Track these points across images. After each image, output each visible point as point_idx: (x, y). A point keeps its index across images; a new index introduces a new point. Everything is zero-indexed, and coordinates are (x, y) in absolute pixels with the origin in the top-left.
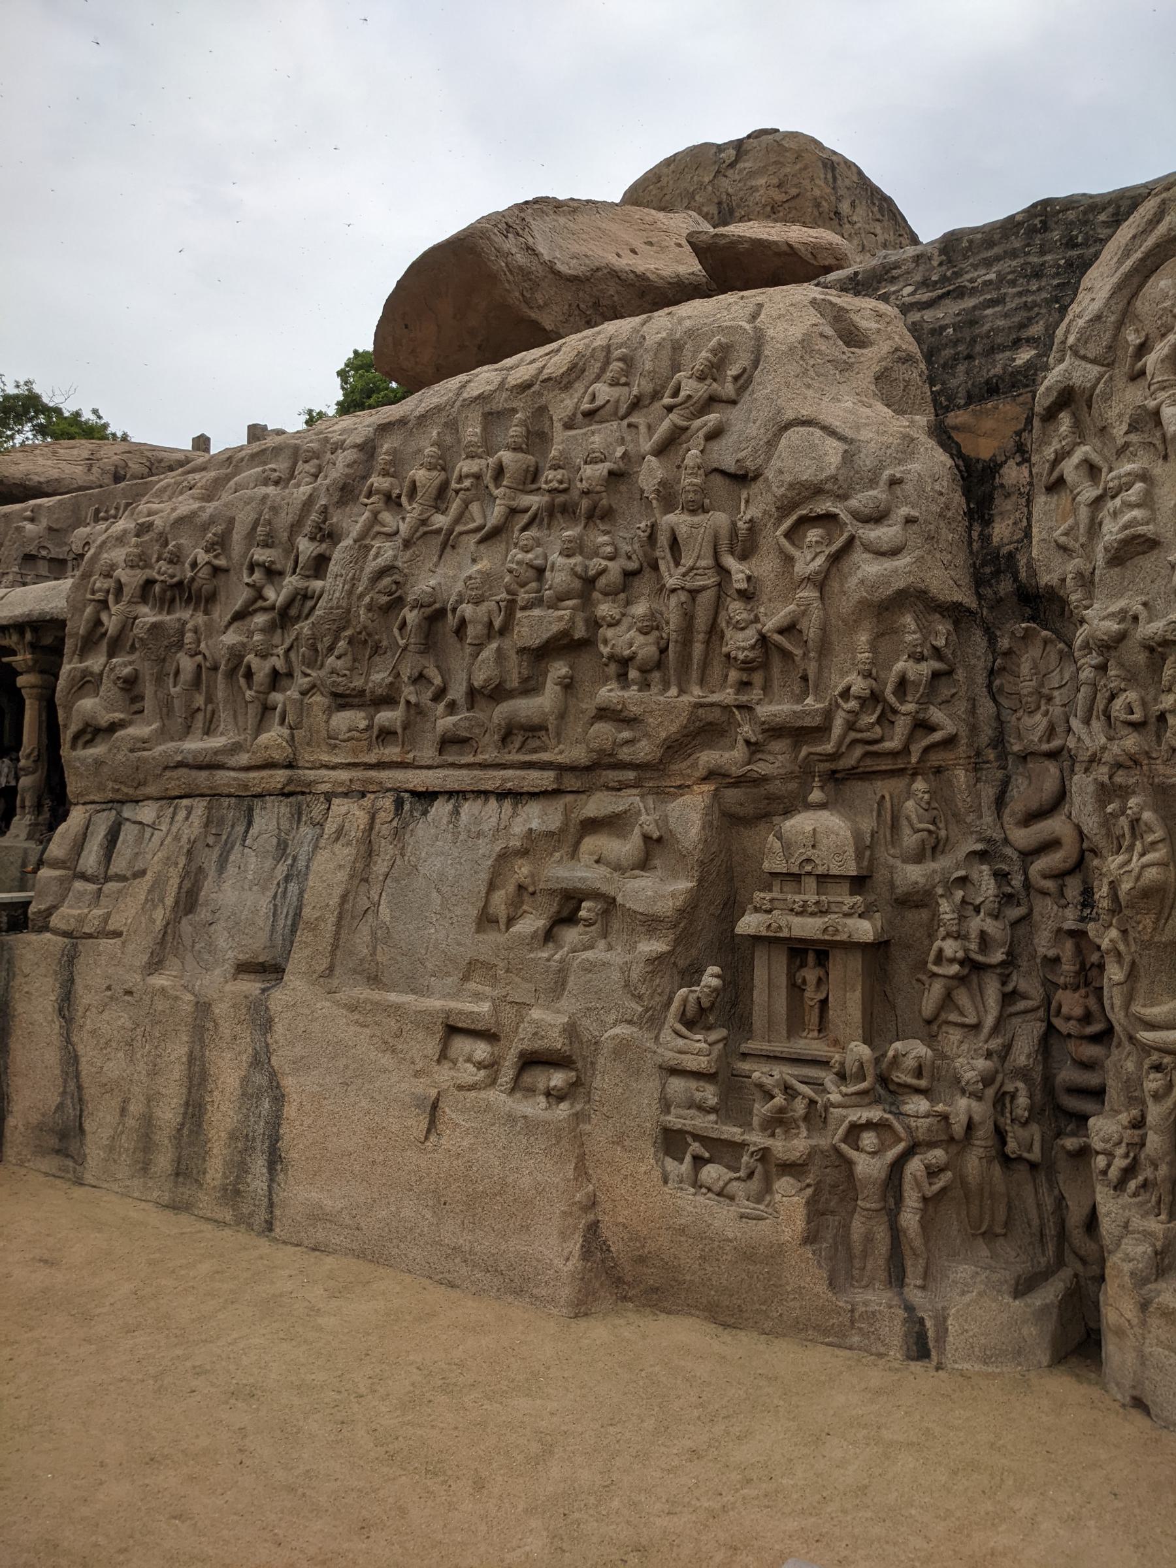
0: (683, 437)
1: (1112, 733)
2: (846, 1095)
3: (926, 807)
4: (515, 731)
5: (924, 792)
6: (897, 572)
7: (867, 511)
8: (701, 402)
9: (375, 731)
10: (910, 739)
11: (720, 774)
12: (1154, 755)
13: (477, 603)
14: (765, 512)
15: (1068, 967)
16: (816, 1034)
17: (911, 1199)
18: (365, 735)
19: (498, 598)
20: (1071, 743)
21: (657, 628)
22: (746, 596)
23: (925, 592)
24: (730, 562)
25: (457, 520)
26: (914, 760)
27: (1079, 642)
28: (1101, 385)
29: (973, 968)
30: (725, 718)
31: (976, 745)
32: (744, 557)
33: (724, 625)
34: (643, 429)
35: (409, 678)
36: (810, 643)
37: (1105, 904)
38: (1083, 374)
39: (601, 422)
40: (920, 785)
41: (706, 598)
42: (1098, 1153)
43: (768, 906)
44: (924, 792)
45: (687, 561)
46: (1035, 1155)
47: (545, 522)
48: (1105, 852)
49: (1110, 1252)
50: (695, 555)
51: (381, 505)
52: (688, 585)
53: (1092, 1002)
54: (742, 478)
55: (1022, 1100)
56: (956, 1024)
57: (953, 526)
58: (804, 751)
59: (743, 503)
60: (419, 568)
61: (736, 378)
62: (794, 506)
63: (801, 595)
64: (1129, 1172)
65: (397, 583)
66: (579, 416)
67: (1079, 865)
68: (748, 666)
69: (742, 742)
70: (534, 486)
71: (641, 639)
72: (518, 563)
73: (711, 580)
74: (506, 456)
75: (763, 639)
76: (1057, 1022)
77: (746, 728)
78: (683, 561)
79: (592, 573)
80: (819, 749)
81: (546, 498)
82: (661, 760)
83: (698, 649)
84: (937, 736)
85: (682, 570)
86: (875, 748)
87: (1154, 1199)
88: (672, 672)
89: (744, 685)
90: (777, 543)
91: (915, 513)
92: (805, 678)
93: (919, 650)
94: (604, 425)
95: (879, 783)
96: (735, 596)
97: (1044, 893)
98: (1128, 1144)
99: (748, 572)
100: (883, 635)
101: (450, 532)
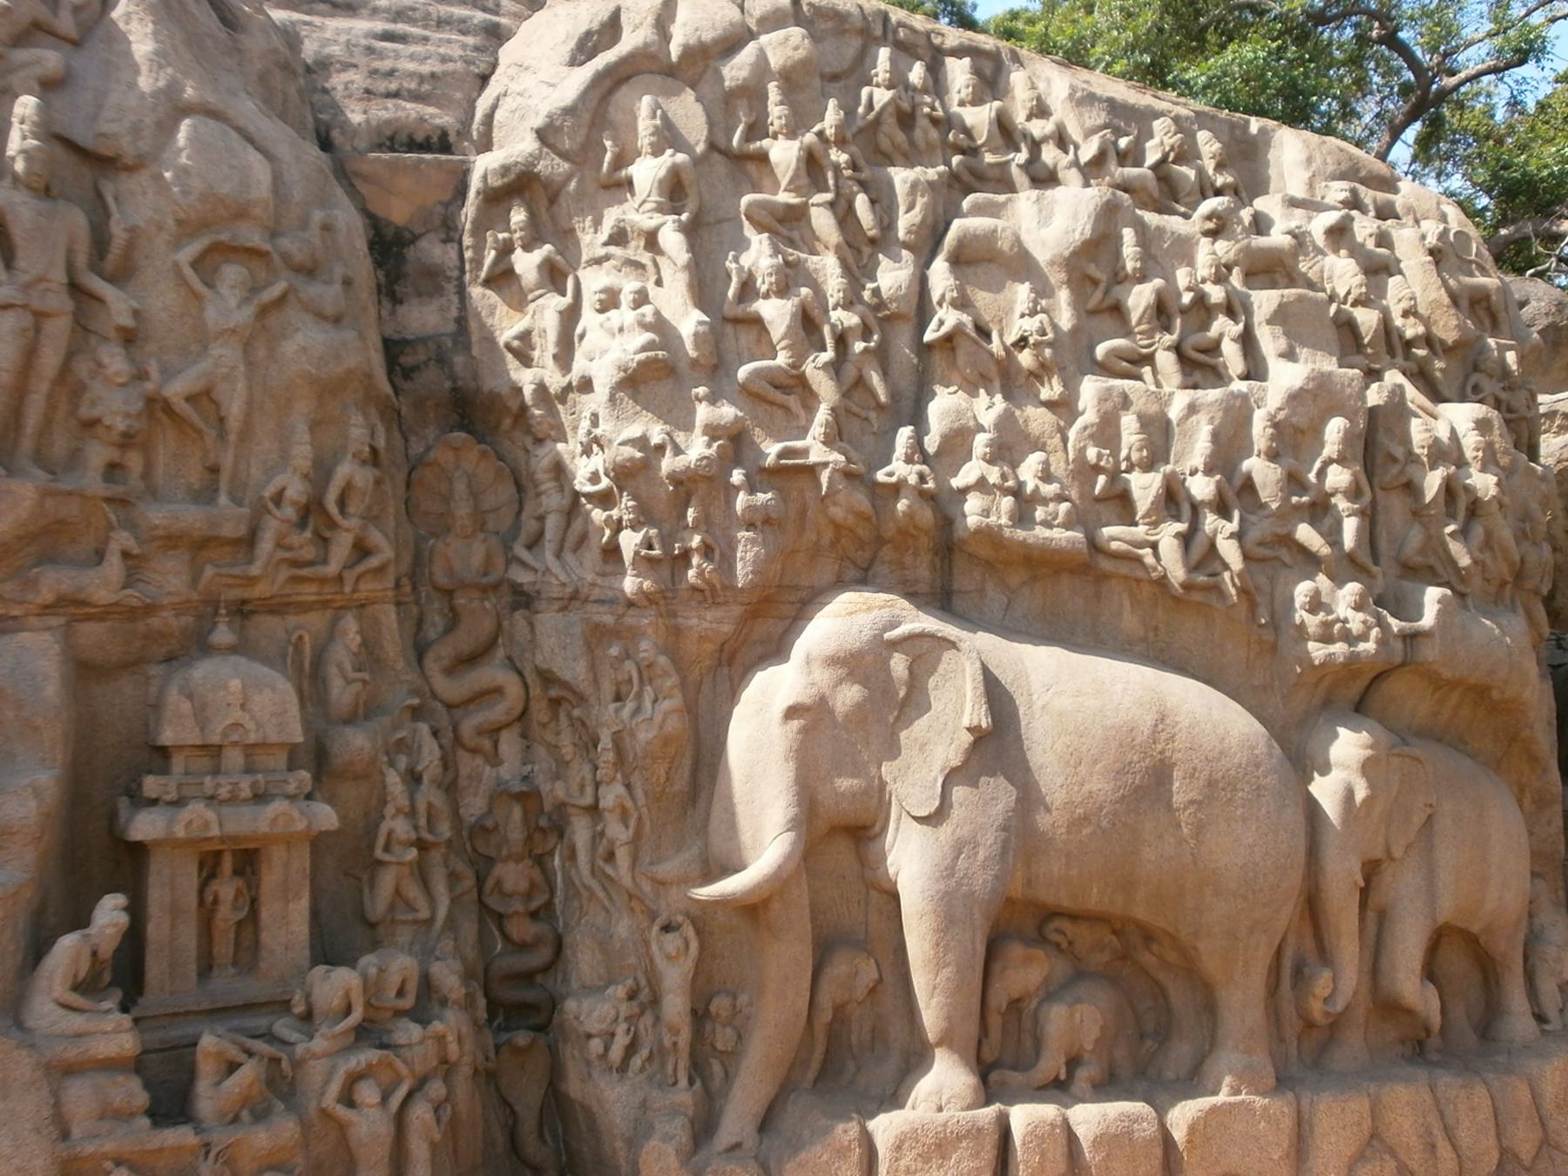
1: (609, 568)
2: (334, 1037)
7: (299, 257)
12: (670, 595)
15: (516, 834)
16: (232, 970)
17: (419, 1150)
20: (523, 577)
26: (347, 589)
27: (546, 462)
28: (573, 185)
29: (422, 845)
32: (112, 279)
37: (610, 756)
38: (552, 166)
42: (589, 1036)
43: (173, 796)
46: (490, 1065)
48: (592, 700)
49: (634, 1143)
52: (36, 304)
53: (536, 874)
55: (482, 1002)
56: (404, 922)
62: (203, 226)
64: (631, 1049)
67: (524, 714)
68: (127, 441)
69: (118, 554)
75: (157, 406)
76: (493, 902)
77: (125, 534)
78: (21, 263)
80: (236, 571)
85: (26, 278)
86: (305, 572)
87: (670, 1068)
89: (113, 470)
92: (214, 470)
95: (293, 620)
96: (112, 334)
97: (474, 751)
98: (627, 1019)
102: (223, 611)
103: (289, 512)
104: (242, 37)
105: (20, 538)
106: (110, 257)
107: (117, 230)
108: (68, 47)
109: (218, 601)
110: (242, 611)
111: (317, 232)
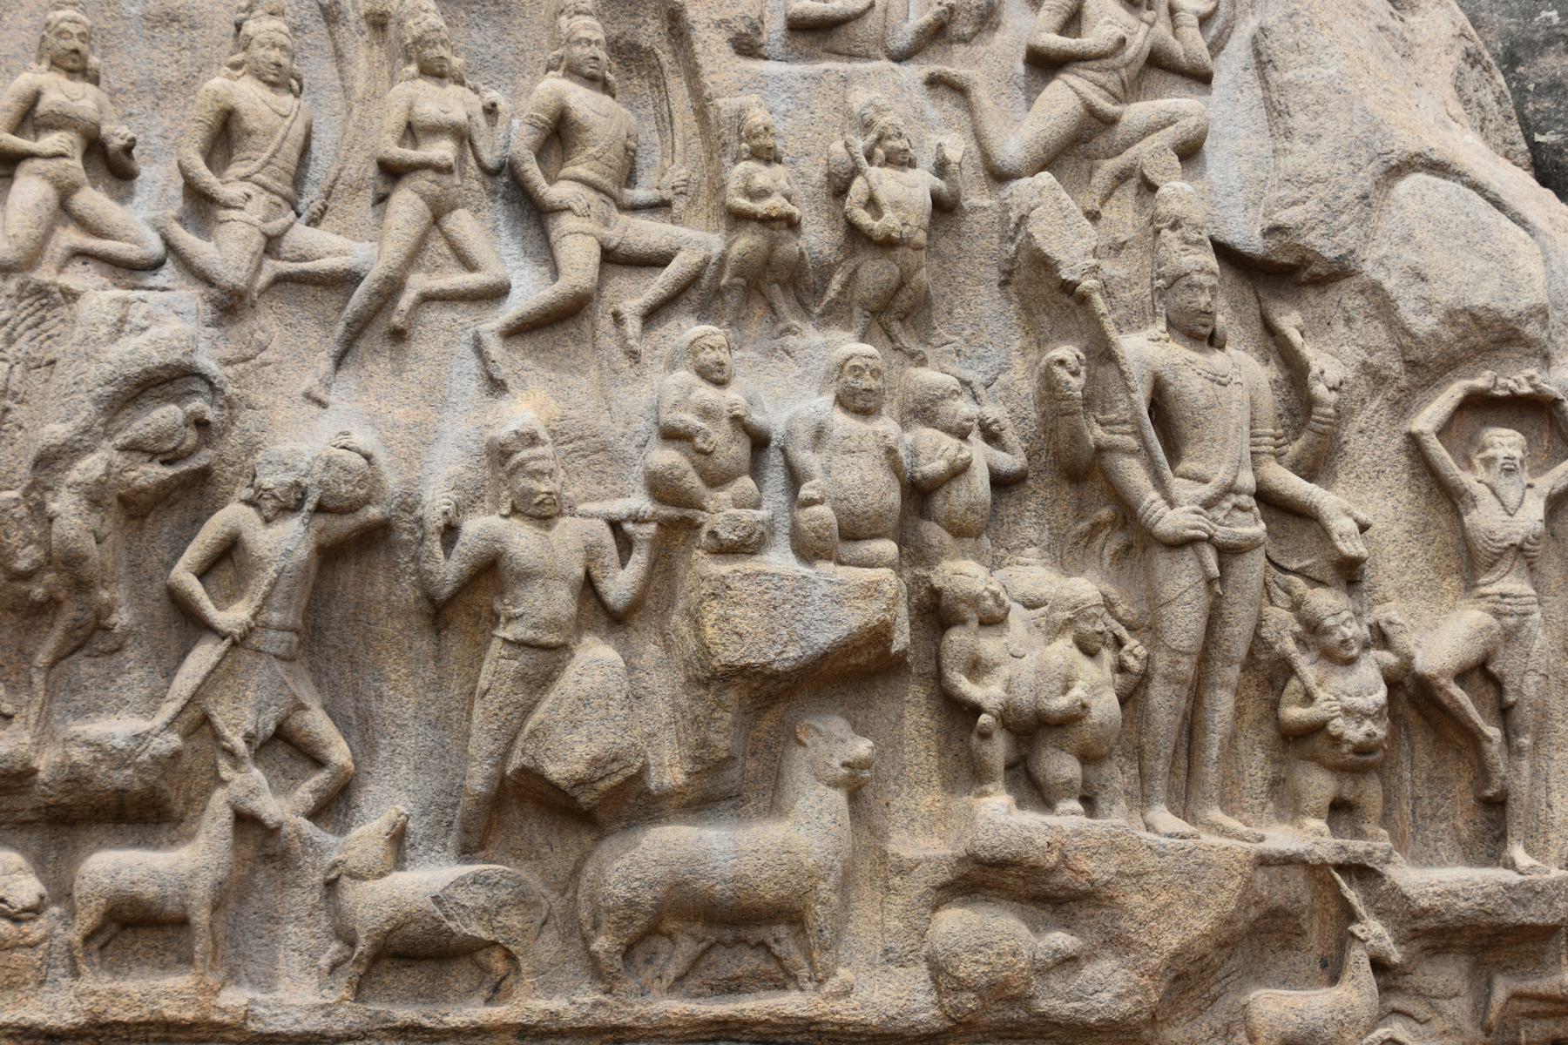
0: (1102, 142)
4: (670, 925)
8: (1141, 62)
9: (87, 919)
13: (543, 514)
18: (35, 930)
19: (619, 507)
22: (1349, 573)
25: (414, 257)
32: (1310, 475)
33: (1290, 645)
34: (981, 94)
35: (249, 738)
36: (1526, 714)
39: (851, 56)
41: (1253, 568)
47: (732, 300)
51: (74, 166)
52: (1221, 533)
54: (1273, 273)
58: (1502, 989)
59: (1296, 338)
60: (268, 384)
61: (1204, 20)
65: (201, 424)
66: (774, 29)
68: (1361, 762)
70: (640, 194)
71: (1085, 664)
72: (706, 413)
73: (1259, 529)
74: (583, 101)
75: (1411, 694)
79: (934, 466)
81: (747, 242)
83: (1222, 705)
85: (1206, 491)
88: (1161, 766)
89: (1340, 810)
94: (861, 66)
96: (1329, 575)
99: (1363, 516)
101: (391, 289)
104: (1411, 19)
105: (1221, 946)
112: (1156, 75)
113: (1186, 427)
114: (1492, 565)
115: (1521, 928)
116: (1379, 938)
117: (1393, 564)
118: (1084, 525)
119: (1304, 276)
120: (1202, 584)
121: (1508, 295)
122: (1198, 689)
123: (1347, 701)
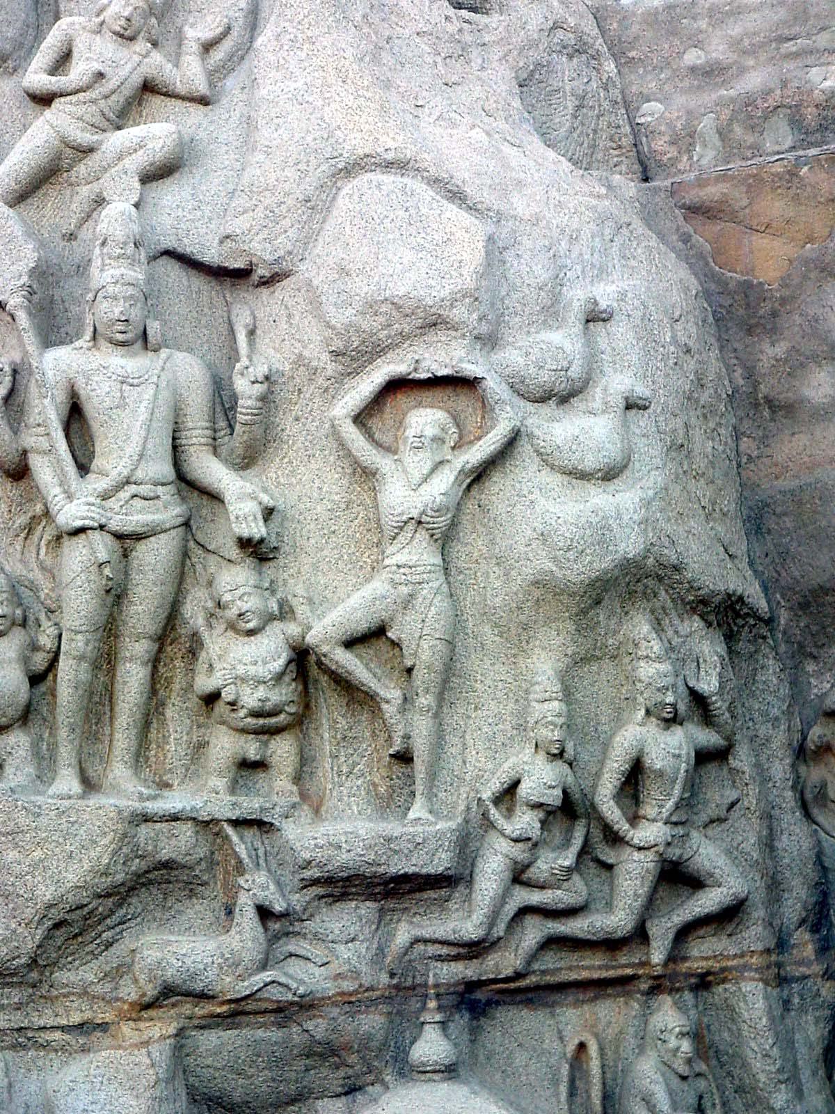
0: (81, 169)
3: (683, 1069)
5: (682, 1034)
6: (622, 517)
7: (545, 377)
8: (127, 91)
10: (650, 906)
11: (188, 994)
14: (300, 361)
21: (24, 624)
22: (257, 551)
23: (676, 568)
24: (212, 470)
26: (657, 956)
30: (202, 852)
31: (777, 922)
33: (199, 621)
40: (669, 1017)
44: (682, 1034)
45: (113, 460)
50: (132, 449)
57: (711, 425)
58: (403, 934)
59: (242, 338)
62: (374, 351)
63: (401, 558)
68: (266, 724)
69: (251, 913)
75: (302, 660)
77: (261, 877)
78: (97, 463)
82: (33, 963)
83: (132, 678)
84: (708, 901)
85: (102, 484)
89: (249, 767)
90: (335, 432)
91: (641, 390)
92: (404, 758)
93: (670, 699)
96: (234, 552)
99: (266, 499)
100: (585, 660)
102: (432, 1004)
103: (526, 821)
106: (238, 428)
107: (245, 388)
108: (194, 108)
109: (425, 985)
110: (474, 1002)
111: (579, 327)
112: (157, 101)
113: (95, 426)
114: (394, 538)
115: (405, 878)
116: (264, 888)
117: (312, 541)
118: (22, 520)
119: (255, 278)
120: (94, 569)
121: (433, 283)
122: (106, 660)
123: (241, 670)
